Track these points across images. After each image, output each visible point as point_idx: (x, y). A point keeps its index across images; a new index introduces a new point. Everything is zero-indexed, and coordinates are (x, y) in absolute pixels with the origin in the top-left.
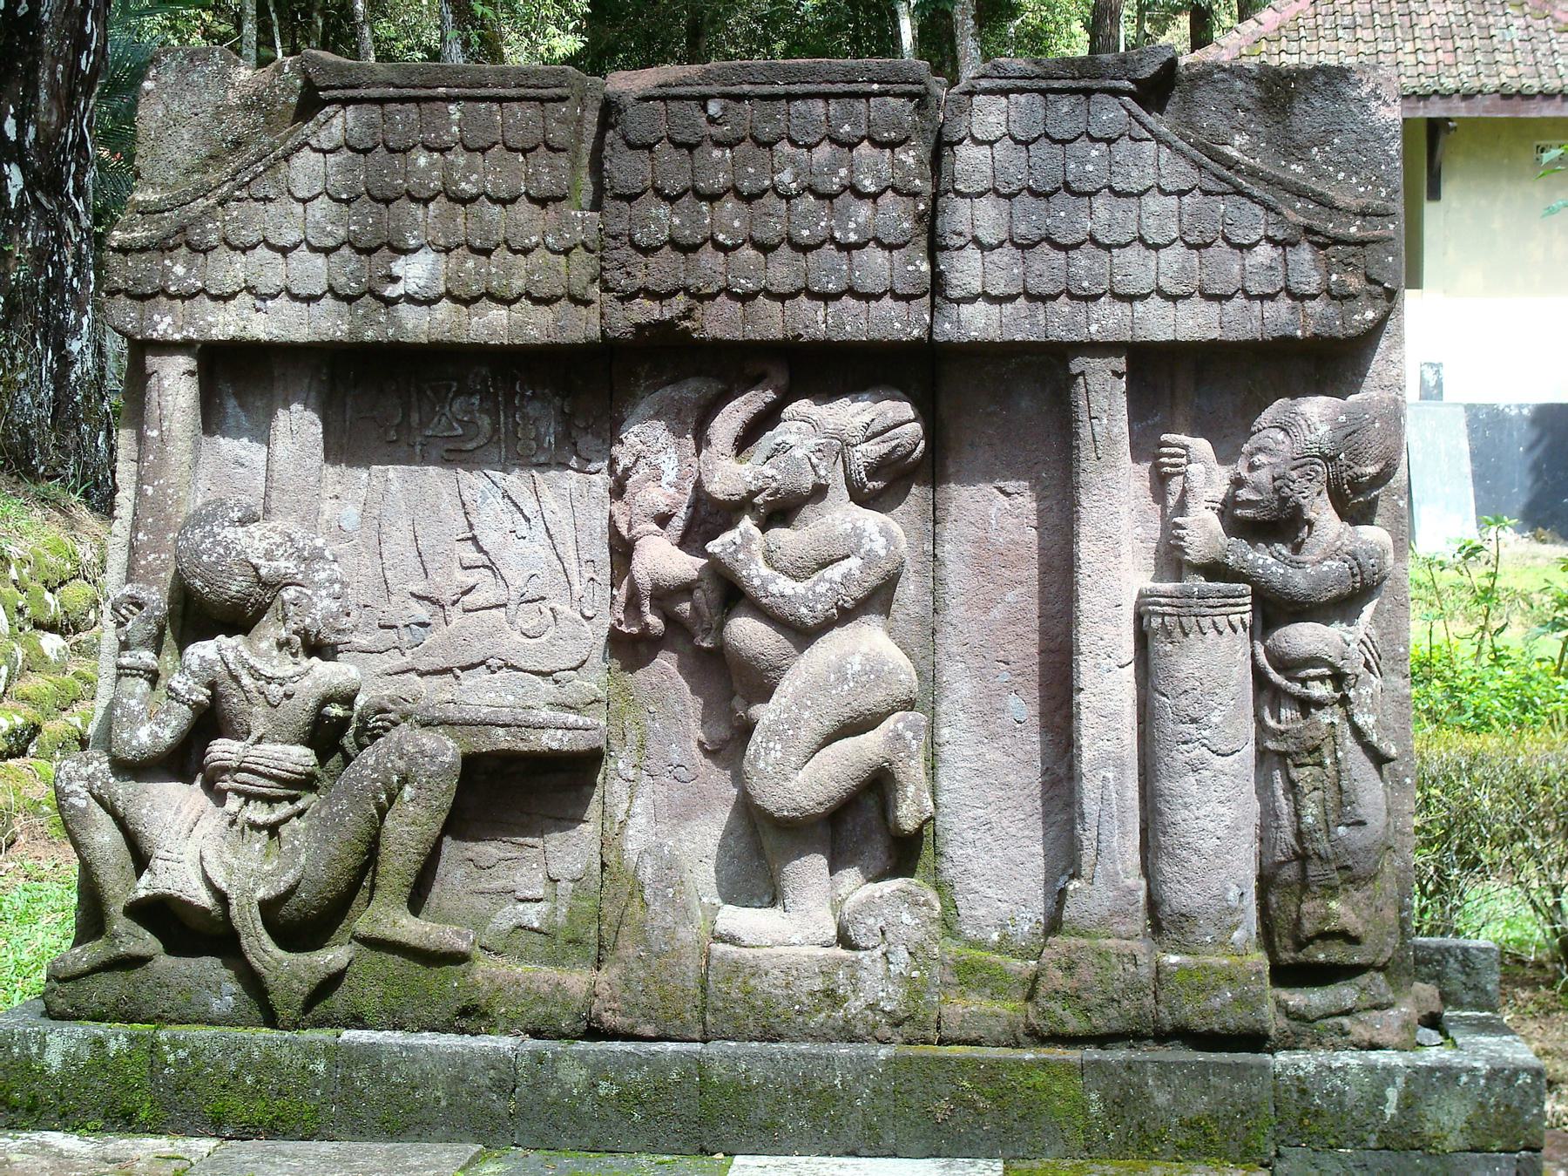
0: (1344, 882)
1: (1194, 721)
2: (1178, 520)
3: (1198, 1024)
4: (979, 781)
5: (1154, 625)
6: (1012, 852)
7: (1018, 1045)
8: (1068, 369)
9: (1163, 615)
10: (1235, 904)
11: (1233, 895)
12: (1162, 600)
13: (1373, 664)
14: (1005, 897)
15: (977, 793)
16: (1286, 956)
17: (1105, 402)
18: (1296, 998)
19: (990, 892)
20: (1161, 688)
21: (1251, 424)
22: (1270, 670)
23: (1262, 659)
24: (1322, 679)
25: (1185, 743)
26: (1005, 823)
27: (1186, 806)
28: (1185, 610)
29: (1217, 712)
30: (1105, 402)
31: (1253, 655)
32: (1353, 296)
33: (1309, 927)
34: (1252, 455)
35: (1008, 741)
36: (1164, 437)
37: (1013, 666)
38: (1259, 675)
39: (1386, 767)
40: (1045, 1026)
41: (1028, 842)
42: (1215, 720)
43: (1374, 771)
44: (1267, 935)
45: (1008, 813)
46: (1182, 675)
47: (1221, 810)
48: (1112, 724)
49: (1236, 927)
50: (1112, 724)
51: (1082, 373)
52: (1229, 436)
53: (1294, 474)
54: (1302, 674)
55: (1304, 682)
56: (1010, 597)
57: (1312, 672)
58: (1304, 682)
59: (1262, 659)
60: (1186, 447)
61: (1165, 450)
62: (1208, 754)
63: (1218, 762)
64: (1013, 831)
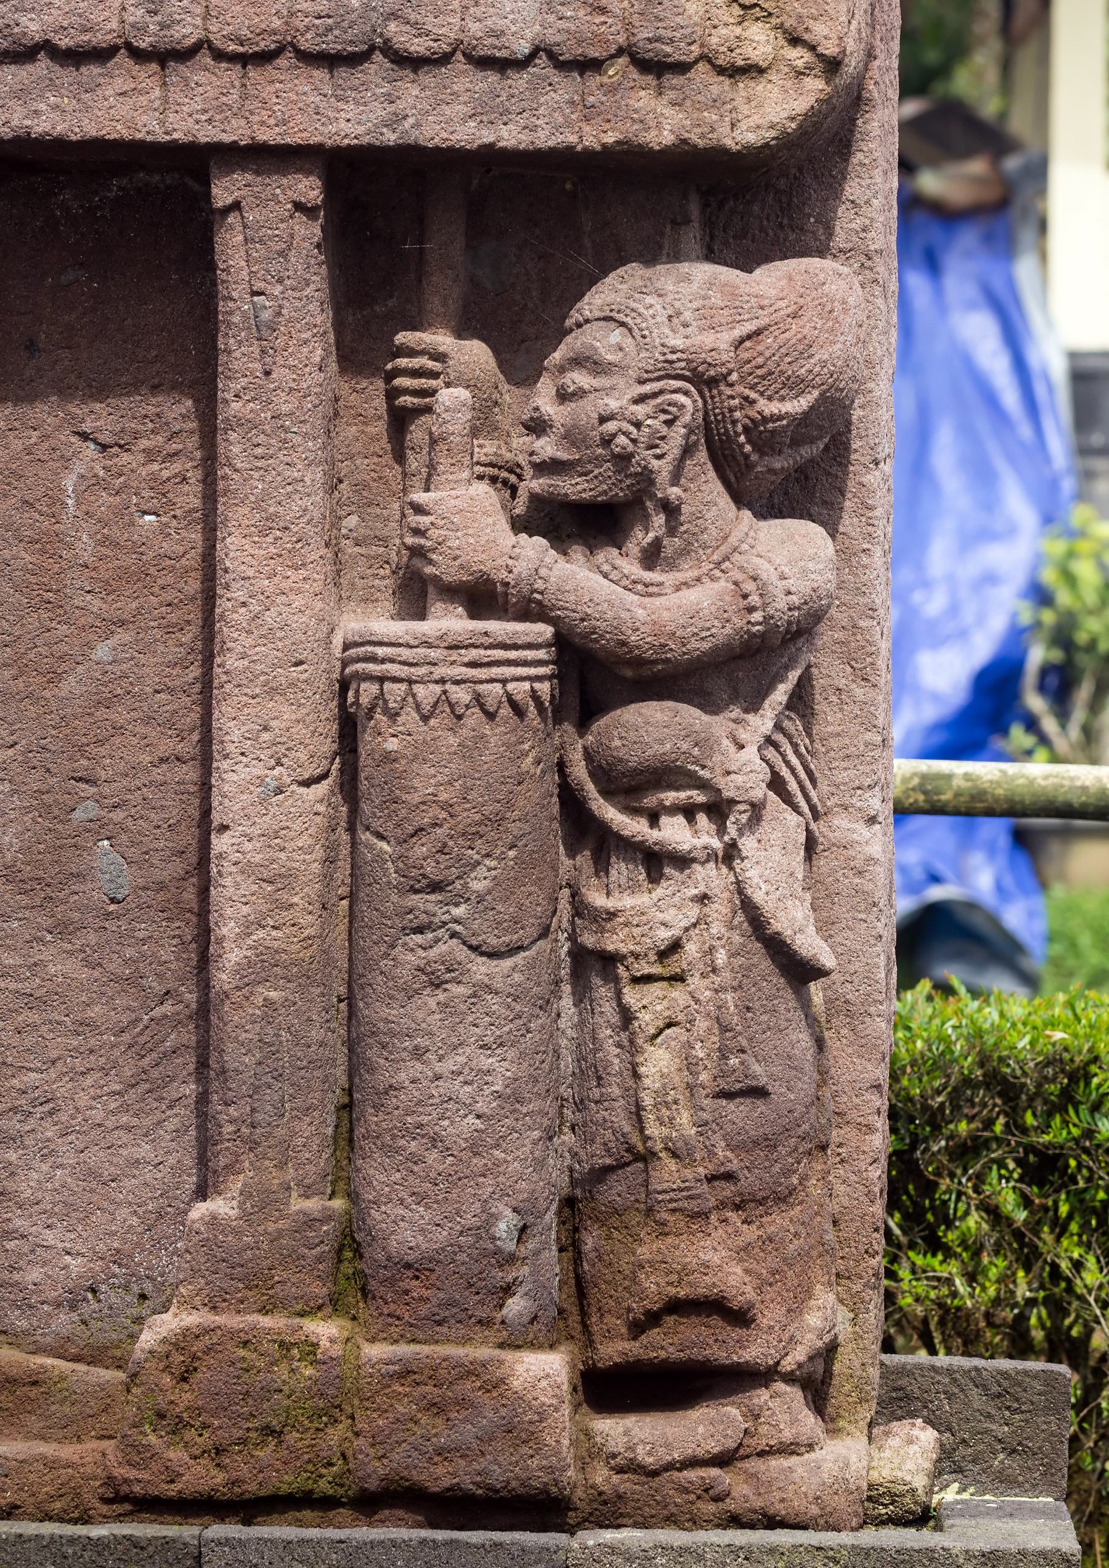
0: (722, 1205)
1: (435, 887)
2: (419, 497)
3: (440, 1477)
4: (34, 1017)
5: (365, 700)
6: (95, 1157)
7: (85, 1520)
8: (208, 196)
9: (381, 680)
10: (510, 1246)
11: (505, 1226)
12: (381, 651)
13: (793, 786)
14: (79, 1247)
15: (29, 1040)
16: (614, 1349)
17: (272, 262)
18: (617, 1430)
19: (50, 1237)
20: (375, 824)
21: (565, 317)
22: (590, 788)
23: (579, 771)
24: (689, 812)
25: (420, 930)
26: (83, 1100)
27: (418, 1054)
28: (422, 671)
29: (481, 871)
30: (272, 262)
31: (561, 767)
32: (753, 70)
33: (654, 1287)
34: (562, 370)
35: (93, 938)
36: (403, 338)
37: (106, 790)
38: (571, 803)
39: (816, 991)
40: (143, 1480)
41: (125, 1137)
42: (478, 886)
43: (789, 994)
44: (575, 1310)
45: (89, 1081)
46: (416, 798)
47: (487, 1062)
48: (283, 896)
49: (508, 1290)
50: (283, 896)
51: (236, 206)
52: (524, 330)
53: (640, 410)
54: (649, 801)
55: (654, 819)
56: (102, 652)
57: (670, 797)
58: (654, 819)
59: (579, 771)
60: (440, 357)
61: (403, 362)
62: (462, 953)
63: (481, 968)
64: (98, 1115)
